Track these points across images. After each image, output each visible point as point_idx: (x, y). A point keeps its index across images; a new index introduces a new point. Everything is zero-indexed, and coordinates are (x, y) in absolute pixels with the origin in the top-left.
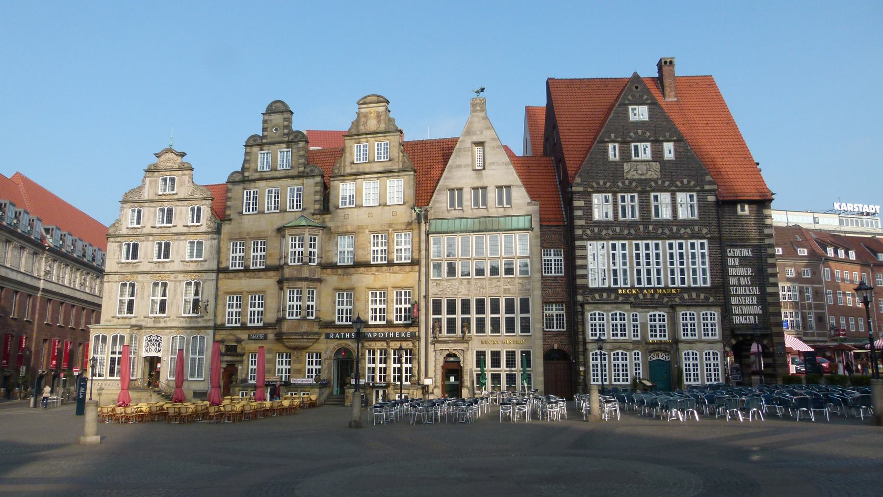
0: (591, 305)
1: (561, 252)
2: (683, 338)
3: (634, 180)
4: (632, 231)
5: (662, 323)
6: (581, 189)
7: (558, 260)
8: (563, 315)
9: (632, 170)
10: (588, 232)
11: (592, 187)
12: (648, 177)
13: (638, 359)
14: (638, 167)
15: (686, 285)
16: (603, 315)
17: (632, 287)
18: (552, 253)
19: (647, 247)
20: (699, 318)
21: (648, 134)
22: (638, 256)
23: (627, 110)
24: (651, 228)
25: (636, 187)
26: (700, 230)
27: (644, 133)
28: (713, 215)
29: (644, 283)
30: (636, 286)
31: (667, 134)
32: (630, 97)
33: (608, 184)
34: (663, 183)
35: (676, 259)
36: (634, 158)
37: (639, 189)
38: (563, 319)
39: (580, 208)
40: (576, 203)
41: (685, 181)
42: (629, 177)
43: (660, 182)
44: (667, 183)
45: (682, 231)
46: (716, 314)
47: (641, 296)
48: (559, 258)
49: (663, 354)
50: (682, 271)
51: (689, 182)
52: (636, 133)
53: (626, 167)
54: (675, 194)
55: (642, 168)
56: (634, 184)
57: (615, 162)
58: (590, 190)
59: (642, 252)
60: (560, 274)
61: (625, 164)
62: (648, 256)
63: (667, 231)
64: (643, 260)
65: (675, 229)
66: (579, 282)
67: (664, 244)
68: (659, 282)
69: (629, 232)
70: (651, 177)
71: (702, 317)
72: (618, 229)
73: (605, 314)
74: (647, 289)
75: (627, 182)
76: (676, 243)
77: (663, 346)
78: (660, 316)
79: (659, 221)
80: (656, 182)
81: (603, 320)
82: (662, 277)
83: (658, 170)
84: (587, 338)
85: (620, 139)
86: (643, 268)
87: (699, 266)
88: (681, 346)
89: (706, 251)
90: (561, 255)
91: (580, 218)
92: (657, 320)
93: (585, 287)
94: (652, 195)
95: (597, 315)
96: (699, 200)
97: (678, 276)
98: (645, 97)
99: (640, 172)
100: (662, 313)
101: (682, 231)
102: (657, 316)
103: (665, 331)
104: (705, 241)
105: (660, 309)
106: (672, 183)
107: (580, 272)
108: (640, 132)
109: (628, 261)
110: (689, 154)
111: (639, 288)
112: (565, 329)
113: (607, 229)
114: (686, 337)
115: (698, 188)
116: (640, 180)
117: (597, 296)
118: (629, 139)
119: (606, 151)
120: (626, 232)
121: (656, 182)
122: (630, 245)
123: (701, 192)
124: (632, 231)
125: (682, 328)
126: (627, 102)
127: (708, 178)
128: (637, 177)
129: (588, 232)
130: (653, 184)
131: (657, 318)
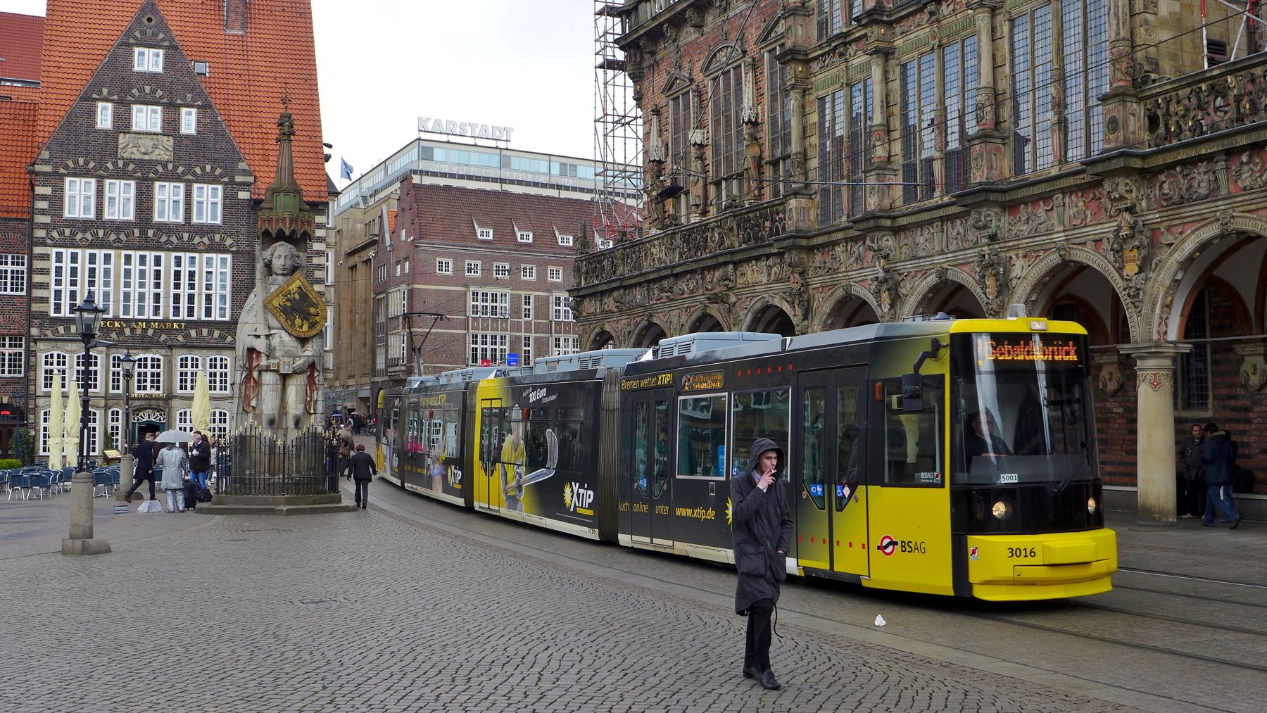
0: (46, 343)
1: (23, 259)
2: (179, 391)
3: (132, 161)
4: (122, 237)
5: (155, 370)
6: (48, 169)
7: (17, 271)
8: (20, 354)
9: (131, 145)
10: (55, 234)
11: (66, 167)
12: (154, 158)
13: (117, 421)
14: (140, 141)
15: (195, 318)
16: (64, 357)
17: (116, 319)
18: (10, 260)
19: (143, 260)
20: (204, 366)
21: (160, 93)
22: (127, 273)
23: (131, 54)
24: (150, 233)
25: (134, 171)
26: (222, 240)
27: (153, 91)
28: (244, 220)
29: (134, 314)
30: (122, 316)
31: (189, 96)
32: (137, 34)
33: (92, 165)
34: (175, 168)
35: (184, 280)
36: (134, 128)
37: (139, 174)
38: (20, 360)
39: (44, 197)
40: (40, 190)
41: (208, 168)
42: (125, 155)
43: (170, 166)
44: (181, 169)
45: (197, 240)
46: (229, 359)
47: (127, 332)
48: (20, 268)
49: (157, 414)
50: (191, 298)
51: (213, 169)
52: (142, 90)
53: (123, 139)
54: (191, 186)
55: (147, 143)
56: (131, 166)
57: (105, 132)
58: (62, 171)
59: (135, 267)
60: (19, 293)
61: (121, 136)
62: (142, 273)
63: (174, 239)
64: (135, 279)
65: (186, 236)
66: (36, 307)
67: (168, 258)
68: (156, 310)
69: (118, 238)
70: (159, 158)
71: (208, 363)
72: (101, 233)
73: (67, 356)
74: (137, 321)
75: (121, 163)
76: (185, 257)
77: (153, 402)
78: (153, 359)
79: (165, 224)
80: (165, 167)
81: (64, 364)
82: (161, 304)
83: (171, 149)
84: (38, 390)
85: (115, 97)
86: (134, 290)
87: (216, 292)
88: (175, 403)
89: (228, 270)
90: (23, 264)
91: (43, 212)
92: (149, 366)
93: (44, 315)
94: (157, 184)
95: (55, 356)
96: (225, 197)
97: (184, 304)
98: (161, 36)
99: (142, 149)
100: (157, 356)
101: (197, 240)
102: (149, 360)
103: (158, 381)
104: (229, 257)
105: (154, 351)
106: (189, 169)
107: (37, 293)
108: (147, 89)
109: (112, 280)
110: (218, 128)
111: (126, 321)
112: (22, 375)
113: (84, 232)
114: (184, 391)
115: (226, 179)
116: (141, 161)
117: (61, 329)
118: (129, 98)
119: (91, 115)
120: (113, 237)
121: (165, 167)
122: (118, 256)
123: (231, 187)
124: (122, 237)
125: (179, 378)
126: (132, 41)
127: (242, 165)
128: (137, 156)
129: (55, 234)
130: (160, 168)
131: (149, 363)
